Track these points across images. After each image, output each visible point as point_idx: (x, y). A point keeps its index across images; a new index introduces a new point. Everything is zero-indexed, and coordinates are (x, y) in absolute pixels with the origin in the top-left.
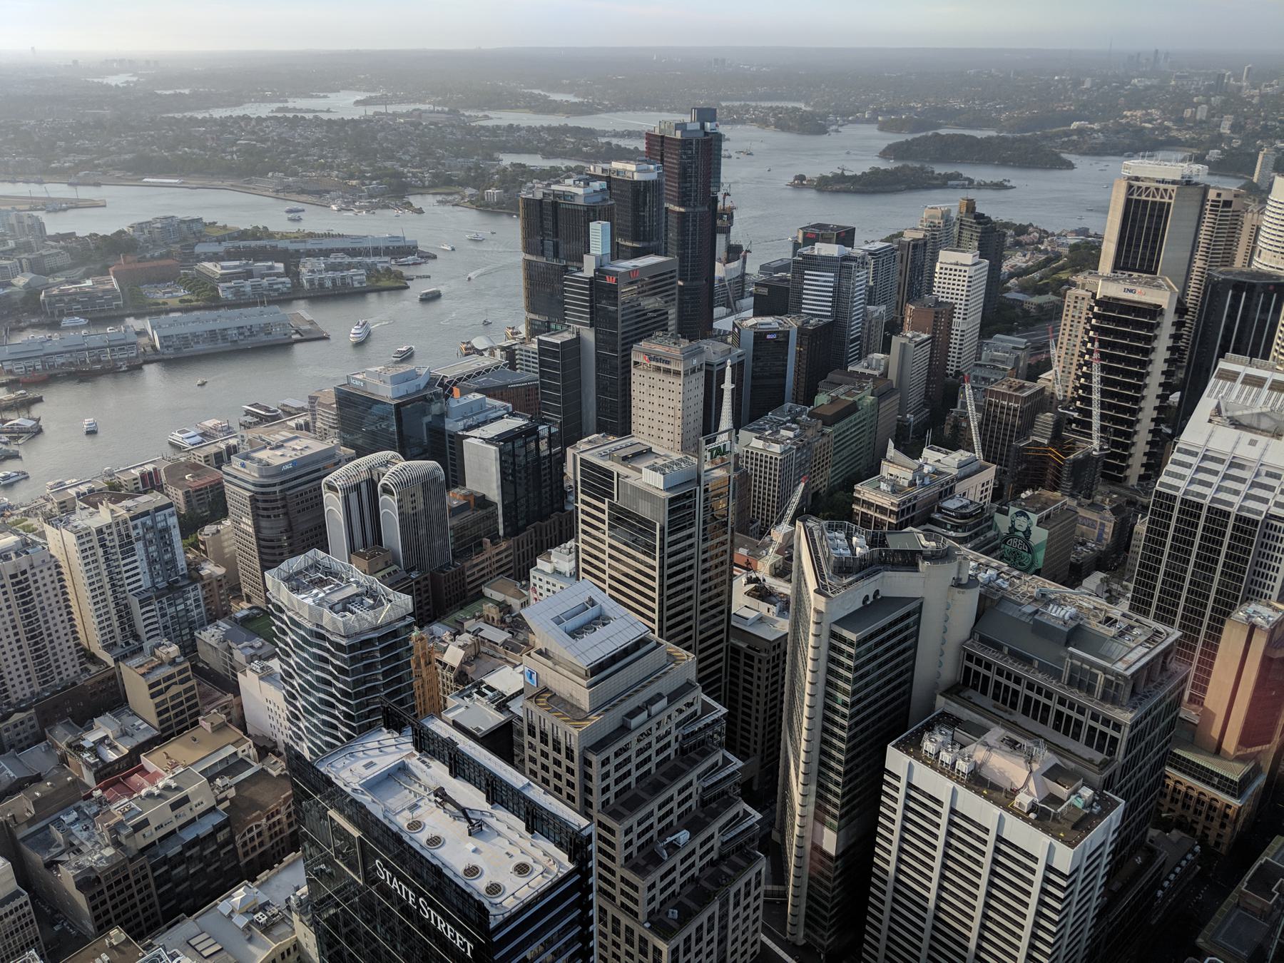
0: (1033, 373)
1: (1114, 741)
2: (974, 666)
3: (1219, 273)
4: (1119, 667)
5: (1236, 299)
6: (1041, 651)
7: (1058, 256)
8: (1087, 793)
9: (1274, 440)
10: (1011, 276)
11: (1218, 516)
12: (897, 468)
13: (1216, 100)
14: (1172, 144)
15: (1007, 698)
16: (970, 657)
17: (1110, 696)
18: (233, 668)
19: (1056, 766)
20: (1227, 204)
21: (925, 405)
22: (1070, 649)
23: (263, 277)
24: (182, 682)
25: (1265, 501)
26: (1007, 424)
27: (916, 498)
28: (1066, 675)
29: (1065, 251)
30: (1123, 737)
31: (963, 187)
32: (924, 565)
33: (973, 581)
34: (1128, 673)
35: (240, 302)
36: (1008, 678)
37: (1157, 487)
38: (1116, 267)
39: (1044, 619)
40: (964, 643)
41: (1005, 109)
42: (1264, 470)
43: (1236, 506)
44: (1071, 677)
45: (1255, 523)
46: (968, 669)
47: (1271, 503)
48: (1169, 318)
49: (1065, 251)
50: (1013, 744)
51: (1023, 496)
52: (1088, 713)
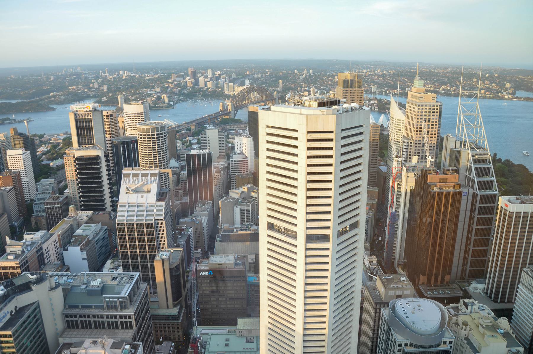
0: (61, 192)
1: (130, 322)
2: (70, 319)
3: (115, 141)
4: (122, 295)
5: (124, 147)
6: (93, 301)
7: (58, 144)
8: (127, 347)
9: (148, 194)
10: (43, 154)
12: (13, 247)
13: (100, 80)
14: (88, 97)
15: (86, 326)
16: (67, 316)
17: (123, 306)
19: (114, 342)
20: (111, 115)
21: (20, 216)
22: (104, 296)
25: (153, 215)
26: (57, 214)
27: (26, 257)
28: (105, 306)
29: (61, 141)
30: (133, 319)
31: (12, 123)
32: (34, 287)
33: (58, 285)
36: (85, 317)
37: (117, 222)
38: (79, 144)
39: (90, 288)
40: (63, 311)
41: (22, 90)
42: (149, 205)
43: (144, 221)
44: (108, 306)
45: (152, 224)
46: (68, 321)
47: (155, 215)
48: (103, 159)
49: (61, 141)
50: (95, 342)
51: (72, 241)
52: (118, 317)
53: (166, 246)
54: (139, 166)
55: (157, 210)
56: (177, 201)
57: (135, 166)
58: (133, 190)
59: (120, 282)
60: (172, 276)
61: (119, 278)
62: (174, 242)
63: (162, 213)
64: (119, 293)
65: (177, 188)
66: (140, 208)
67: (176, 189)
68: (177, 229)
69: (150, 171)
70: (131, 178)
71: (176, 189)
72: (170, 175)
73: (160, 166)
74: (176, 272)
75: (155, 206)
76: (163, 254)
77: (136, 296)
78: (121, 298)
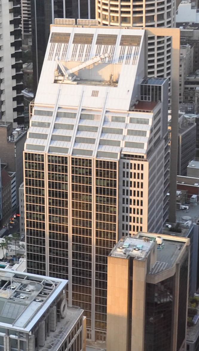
9: (112, 89)
11: (81, 165)
25: (117, 143)
34: (28, 329)
37: (26, 150)
42: (109, 116)
43: (95, 154)
45: (113, 165)
47: (122, 144)
53: (145, 225)
54: (93, 17)
55: (130, 132)
56: (187, 112)
57: (84, 16)
58: (72, 75)
59: (17, 294)
60: (150, 306)
61: (15, 285)
62: (167, 219)
63: (144, 140)
64: (12, 321)
65: (192, 78)
66: (86, 123)
67: (187, 82)
68: (180, 187)
69: (120, 31)
70: (71, 45)
71: (187, 82)
72: (176, 44)
73: (149, 19)
74: (163, 294)
75: (127, 120)
76: (137, 244)
77: (52, 334)
78: (15, 332)
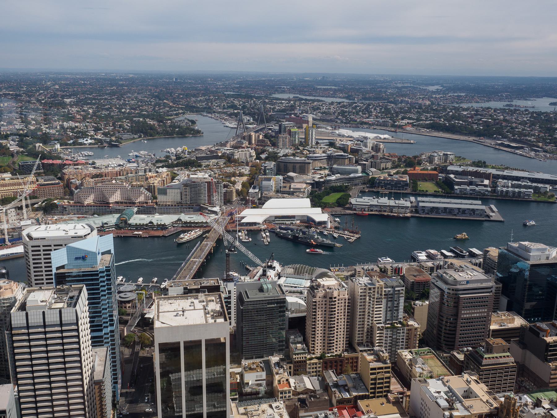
18: (411, 376)
23: (477, 185)
24: (386, 372)
35: (463, 196)
